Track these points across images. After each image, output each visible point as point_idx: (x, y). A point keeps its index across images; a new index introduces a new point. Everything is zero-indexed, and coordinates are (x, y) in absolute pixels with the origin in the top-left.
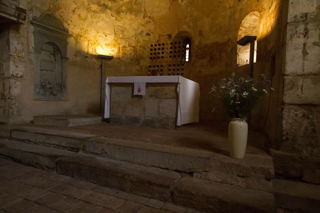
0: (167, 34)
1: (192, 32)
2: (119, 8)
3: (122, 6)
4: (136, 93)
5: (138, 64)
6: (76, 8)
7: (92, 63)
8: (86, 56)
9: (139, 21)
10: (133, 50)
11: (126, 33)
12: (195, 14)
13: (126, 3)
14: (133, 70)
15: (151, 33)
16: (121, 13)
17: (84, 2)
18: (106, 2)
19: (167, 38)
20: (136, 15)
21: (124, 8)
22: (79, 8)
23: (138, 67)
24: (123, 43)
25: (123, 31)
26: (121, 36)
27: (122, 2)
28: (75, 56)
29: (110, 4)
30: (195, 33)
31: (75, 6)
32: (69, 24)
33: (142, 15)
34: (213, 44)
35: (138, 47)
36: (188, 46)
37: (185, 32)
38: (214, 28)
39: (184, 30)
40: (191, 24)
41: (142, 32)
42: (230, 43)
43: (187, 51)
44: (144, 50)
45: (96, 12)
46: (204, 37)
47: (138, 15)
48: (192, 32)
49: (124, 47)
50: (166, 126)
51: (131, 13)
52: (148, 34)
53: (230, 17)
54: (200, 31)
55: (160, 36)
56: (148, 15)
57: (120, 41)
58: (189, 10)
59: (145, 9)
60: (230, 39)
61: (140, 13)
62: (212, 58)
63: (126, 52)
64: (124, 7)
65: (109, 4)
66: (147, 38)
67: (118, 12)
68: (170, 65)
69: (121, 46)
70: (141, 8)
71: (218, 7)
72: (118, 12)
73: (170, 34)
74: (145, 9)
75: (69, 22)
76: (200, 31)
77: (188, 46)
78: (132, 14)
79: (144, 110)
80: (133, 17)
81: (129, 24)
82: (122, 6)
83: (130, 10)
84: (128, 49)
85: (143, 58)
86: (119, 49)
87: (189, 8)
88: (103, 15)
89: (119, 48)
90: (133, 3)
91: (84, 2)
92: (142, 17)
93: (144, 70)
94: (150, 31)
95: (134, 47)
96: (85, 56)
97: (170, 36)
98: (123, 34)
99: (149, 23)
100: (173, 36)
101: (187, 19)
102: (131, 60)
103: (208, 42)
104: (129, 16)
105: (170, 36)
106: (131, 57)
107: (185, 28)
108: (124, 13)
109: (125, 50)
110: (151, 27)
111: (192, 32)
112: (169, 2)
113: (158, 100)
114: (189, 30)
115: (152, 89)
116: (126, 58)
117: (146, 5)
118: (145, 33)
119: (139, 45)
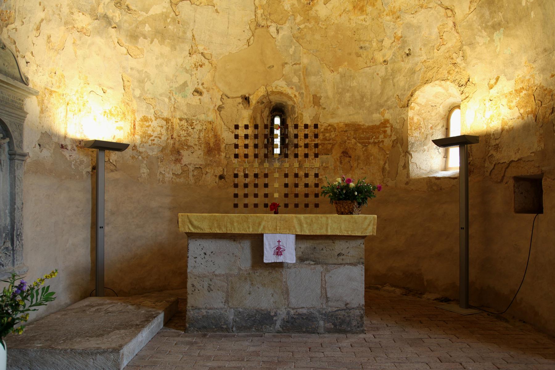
0: (240, 94)
1: (297, 94)
2: (137, 27)
3: (143, 23)
5: (178, 161)
6: (42, 20)
7: (76, 162)
8: (62, 145)
9: (180, 60)
10: (165, 127)
11: (147, 86)
12: (305, 60)
13: (154, 18)
14: (167, 175)
15: (204, 91)
16: (141, 40)
17: (61, 5)
18: (111, 11)
19: (239, 103)
20: (173, 48)
21: (147, 28)
22: (50, 21)
23: (177, 169)
24: (143, 111)
25: (141, 82)
26: (138, 93)
27: (145, 14)
28: (39, 145)
29: (117, 15)
30: (302, 98)
31: (42, 15)
32: (27, 63)
33: (187, 47)
34: (346, 125)
35: (176, 121)
36: (277, 121)
37: (281, 93)
38: (348, 95)
39: (279, 89)
40: (295, 80)
41: (185, 84)
42: (388, 130)
43: (277, 132)
44: (190, 128)
45: (84, 33)
46: (325, 108)
47: (178, 47)
48: (297, 94)
49: (145, 119)
50: (344, 327)
51: (162, 42)
52: (198, 92)
53: (385, 80)
54: (315, 96)
56: (201, 48)
57: (135, 105)
58: (291, 51)
59: (193, 36)
60: (387, 121)
61: (183, 42)
62: (345, 153)
63: (149, 132)
64: (147, 25)
65: (116, 17)
67: (134, 37)
68: (286, 176)
69: (138, 118)
70: (185, 33)
71: (359, 55)
72: (134, 37)
73: (247, 96)
74: (193, 36)
75: (28, 57)
76: (315, 96)
77: (277, 121)
78: (166, 43)
80: (166, 49)
81: (157, 66)
82: (143, 23)
83: (161, 35)
84: (155, 123)
85: (189, 147)
86: (134, 125)
87: (293, 47)
88: (99, 41)
89: (134, 122)
90: (169, 20)
91: (61, 5)
92: (187, 53)
93: (191, 174)
94: (203, 84)
95: (167, 120)
96: (61, 143)
97: (246, 99)
98: (143, 89)
99: (201, 66)
100: (254, 100)
101: (287, 67)
102: (162, 151)
103: (333, 121)
104: (157, 47)
105: (246, 99)
106: (161, 144)
107: (281, 85)
108: (146, 41)
109: (148, 126)
110: (205, 75)
111: (295, 96)
112: (248, 27)
113: (319, 268)
114: (289, 91)
115: (305, 245)
116: (150, 145)
117: (196, 27)
118: (190, 89)
119: (178, 115)
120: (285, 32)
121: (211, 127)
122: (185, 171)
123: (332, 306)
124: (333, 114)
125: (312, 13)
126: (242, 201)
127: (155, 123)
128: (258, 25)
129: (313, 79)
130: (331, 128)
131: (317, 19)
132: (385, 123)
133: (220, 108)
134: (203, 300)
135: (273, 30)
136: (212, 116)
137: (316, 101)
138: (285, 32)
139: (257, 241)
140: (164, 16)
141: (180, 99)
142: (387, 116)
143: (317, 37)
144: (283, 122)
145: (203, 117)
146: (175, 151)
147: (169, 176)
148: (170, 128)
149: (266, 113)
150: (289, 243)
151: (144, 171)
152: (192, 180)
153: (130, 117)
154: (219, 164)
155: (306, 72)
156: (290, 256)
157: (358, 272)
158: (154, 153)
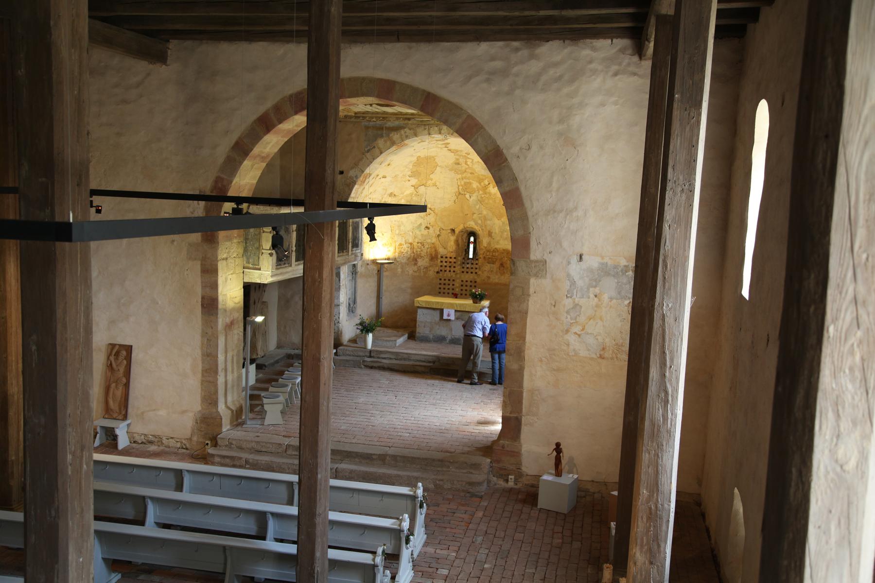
4: (445, 317)
5: (416, 264)
11: (402, 228)
12: (485, 212)
23: (415, 268)
24: (400, 240)
25: (399, 226)
26: (397, 232)
35: (415, 244)
36: (472, 239)
40: (480, 222)
41: (421, 224)
43: (472, 246)
49: (401, 245)
52: (427, 228)
55: (441, 229)
58: (477, 207)
62: (502, 265)
66: (425, 232)
77: (472, 239)
79: (451, 330)
95: (411, 244)
97: (453, 231)
100: (457, 232)
101: (475, 216)
103: (498, 247)
105: (453, 231)
114: (476, 227)
115: (458, 314)
118: (423, 227)
119: (417, 241)
120: (474, 197)
121: (434, 247)
122: (419, 269)
124: (498, 243)
125: (488, 191)
126: (442, 290)
127: (405, 246)
128: (460, 193)
129: (488, 222)
131: (490, 194)
133: (439, 236)
134: (421, 330)
135: (467, 196)
136: (434, 240)
137: (490, 234)
138: (474, 197)
139: (442, 311)
140: (411, 194)
141: (418, 232)
143: (491, 201)
144: (475, 240)
145: (429, 241)
146: (414, 259)
147: (411, 272)
148: (412, 248)
149: (465, 235)
150: (452, 312)
151: (399, 270)
152: (422, 274)
153: (394, 245)
154: (436, 265)
155: (485, 219)
158: (404, 261)
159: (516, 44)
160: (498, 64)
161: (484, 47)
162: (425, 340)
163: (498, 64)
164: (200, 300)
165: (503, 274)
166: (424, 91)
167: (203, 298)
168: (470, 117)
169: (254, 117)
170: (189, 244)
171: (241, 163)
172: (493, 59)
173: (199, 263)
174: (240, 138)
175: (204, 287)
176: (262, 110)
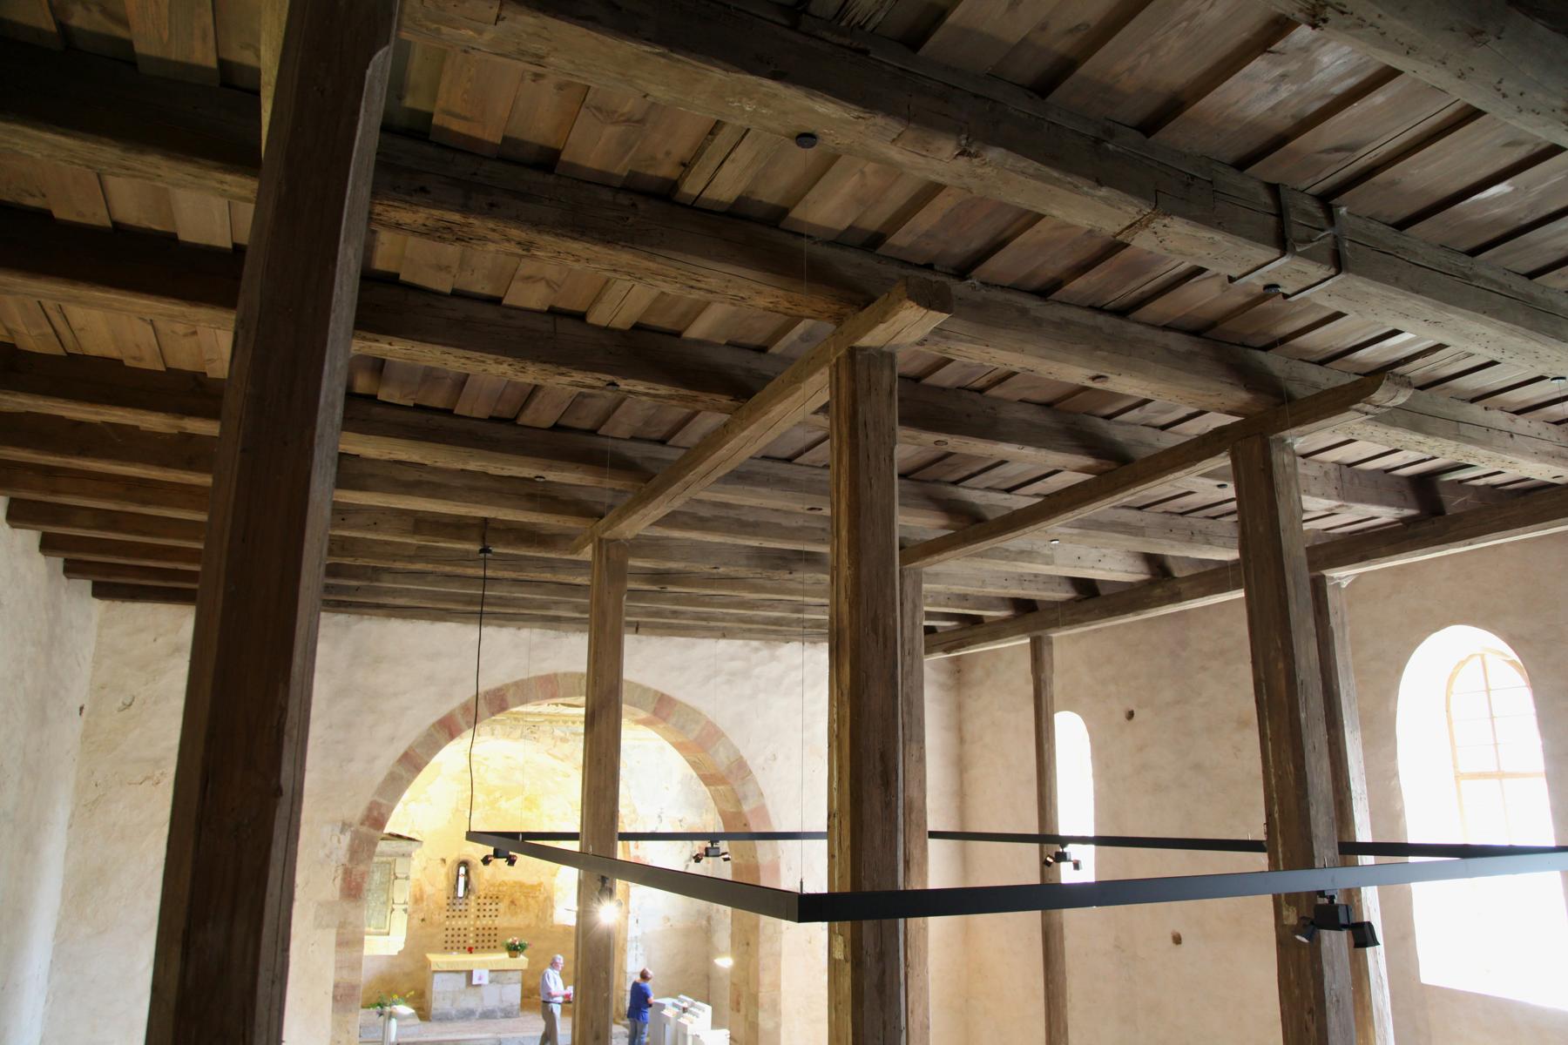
4: (475, 981)
62: (513, 902)
77: (462, 870)
97: (444, 860)
100: (449, 861)
103: (506, 878)
105: (444, 860)
123: (504, 1005)
130: (504, 883)
132: (540, 884)
139: (470, 974)
142: (543, 879)
144: (467, 873)
156: (485, 981)
157: (519, 987)
159: (755, 643)
160: (738, 665)
161: (723, 645)
162: (445, 1018)
163: (738, 665)
164: (330, 989)
165: (514, 914)
166: (656, 692)
167: (336, 986)
168: (708, 722)
169: (435, 719)
170: (320, 904)
171: (409, 782)
172: (732, 659)
173: (334, 931)
174: (410, 747)
175: (339, 967)
176: (443, 711)
